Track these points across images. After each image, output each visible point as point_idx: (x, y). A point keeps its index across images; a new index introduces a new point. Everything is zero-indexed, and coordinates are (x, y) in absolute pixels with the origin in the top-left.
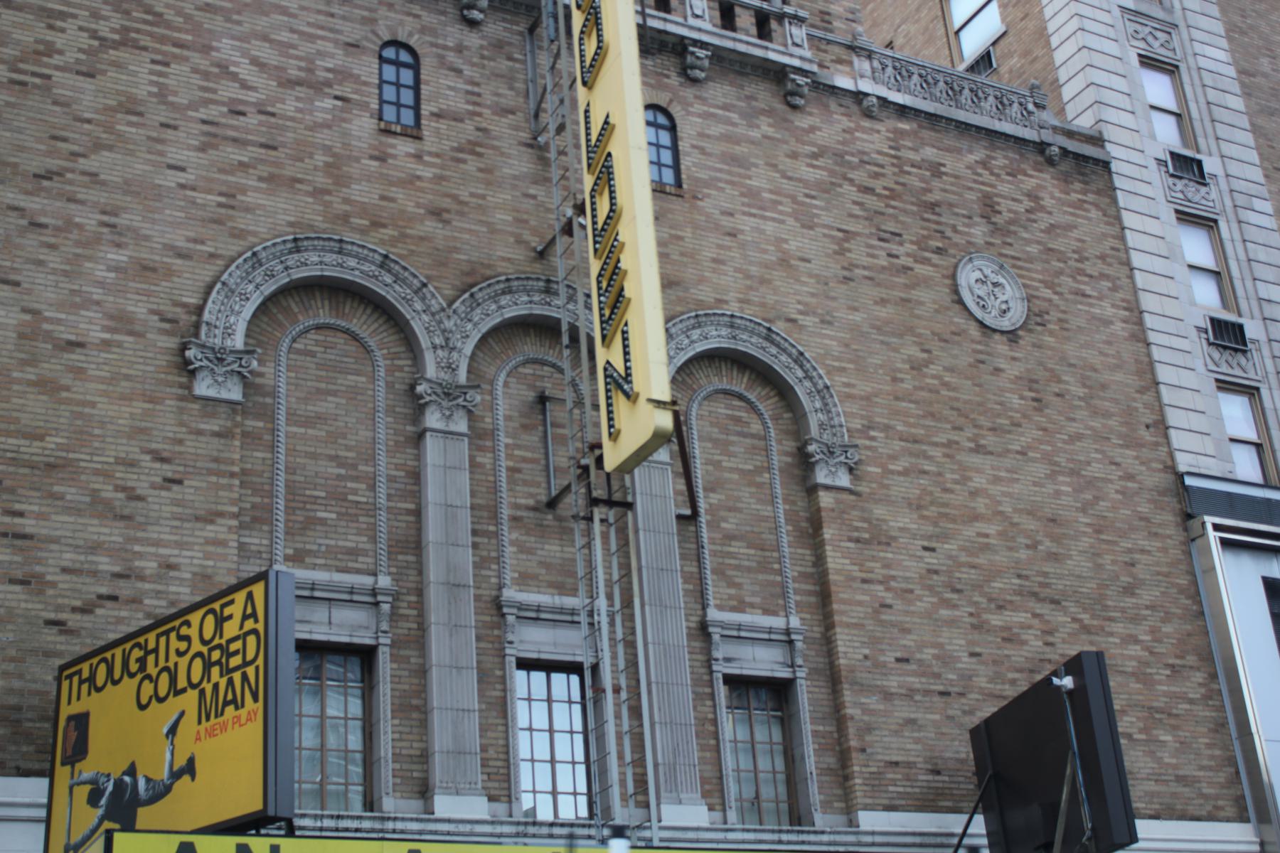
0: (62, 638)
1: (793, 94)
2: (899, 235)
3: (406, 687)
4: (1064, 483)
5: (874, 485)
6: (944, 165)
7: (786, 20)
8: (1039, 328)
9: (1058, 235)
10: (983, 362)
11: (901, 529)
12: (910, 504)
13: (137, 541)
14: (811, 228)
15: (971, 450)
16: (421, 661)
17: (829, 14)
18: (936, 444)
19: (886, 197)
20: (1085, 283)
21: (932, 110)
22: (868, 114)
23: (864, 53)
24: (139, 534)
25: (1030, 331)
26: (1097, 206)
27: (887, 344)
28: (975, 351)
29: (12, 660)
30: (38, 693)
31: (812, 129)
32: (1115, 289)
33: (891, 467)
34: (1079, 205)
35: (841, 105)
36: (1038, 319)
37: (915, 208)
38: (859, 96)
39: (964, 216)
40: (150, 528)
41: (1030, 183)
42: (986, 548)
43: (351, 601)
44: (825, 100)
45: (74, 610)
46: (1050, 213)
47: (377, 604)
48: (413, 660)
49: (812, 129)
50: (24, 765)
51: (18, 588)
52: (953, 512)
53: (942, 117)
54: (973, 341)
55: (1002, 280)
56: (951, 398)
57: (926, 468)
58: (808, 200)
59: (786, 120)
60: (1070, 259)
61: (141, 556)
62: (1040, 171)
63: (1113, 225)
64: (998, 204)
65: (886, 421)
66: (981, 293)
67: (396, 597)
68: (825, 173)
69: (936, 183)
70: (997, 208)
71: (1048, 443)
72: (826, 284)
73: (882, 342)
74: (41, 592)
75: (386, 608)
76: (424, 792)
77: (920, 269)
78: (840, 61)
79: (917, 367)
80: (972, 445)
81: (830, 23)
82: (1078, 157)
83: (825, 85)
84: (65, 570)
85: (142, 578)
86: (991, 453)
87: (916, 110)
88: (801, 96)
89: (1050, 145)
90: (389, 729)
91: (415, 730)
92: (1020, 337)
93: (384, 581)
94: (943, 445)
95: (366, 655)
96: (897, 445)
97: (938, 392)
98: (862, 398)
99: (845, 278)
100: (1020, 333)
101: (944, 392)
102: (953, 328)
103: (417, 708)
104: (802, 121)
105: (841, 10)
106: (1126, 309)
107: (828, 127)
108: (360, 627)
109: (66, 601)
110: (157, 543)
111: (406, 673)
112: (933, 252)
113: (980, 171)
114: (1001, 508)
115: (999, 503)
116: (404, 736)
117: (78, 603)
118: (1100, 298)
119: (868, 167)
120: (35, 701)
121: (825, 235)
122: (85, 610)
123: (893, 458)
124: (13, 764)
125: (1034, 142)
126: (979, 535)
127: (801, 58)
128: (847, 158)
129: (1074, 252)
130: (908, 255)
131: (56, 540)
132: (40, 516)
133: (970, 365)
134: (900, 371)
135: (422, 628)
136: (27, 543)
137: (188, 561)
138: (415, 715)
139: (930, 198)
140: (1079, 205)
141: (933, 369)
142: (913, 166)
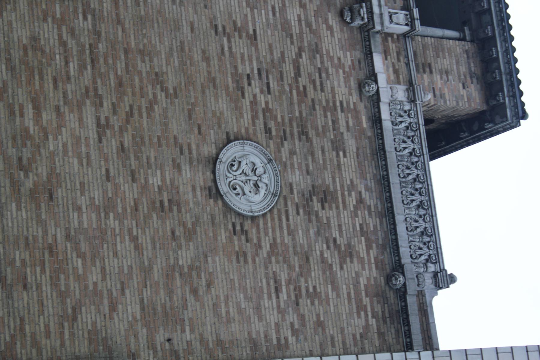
1: (351, 10)
2: (269, 93)
4: (90, 220)
5: (44, 7)
6: (345, 156)
7: (407, 13)
8: (230, 227)
9: (324, 273)
10: (182, 153)
11: (10, 23)
12: (34, 39)
14: (248, 5)
15: (98, 119)
17: (431, 72)
18: (95, 82)
19: (298, 88)
20: (289, 296)
21: (387, 148)
22: (361, 86)
23: (411, 94)
25: (225, 216)
26: (367, 326)
27: (172, 55)
28: (189, 145)
31: (330, 28)
32: (295, 332)
33: (64, 28)
34: (361, 308)
35: (359, 62)
36: (238, 228)
37: (297, 114)
38: (373, 77)
39: (307, 166)
41: (361, 247)
42: (12, 113)
44: (358, 47)
46: (342, 268)
49: (330, 28)
52: (37, 83)
53: (385, 160)
54: (198, 146)
55: (262, 192)
56: (140, 108)
57: (71, 65)
58: (270, 8)
59: (329, 5)
60: (306, 282)
62: (377, 267)
63: (355, 344)
64: (331, 208)
65: (103, 34)
66: (243, 166)
68: (298, 32)
69: (328, 145)
70: (326, 205)
71: (124, 209)
72: (206, 7)
73: (171, 49)
77: (246, 103)
78: (396, 72)
79: (158, 79)
80: (103, 122)
81: (424, 72)
82: (405, 310)
83: (370, 45)
86: (100, 141)
87: (382, 133)
88: (351, 19)
89: (404, 275)
92: (215, 201)
94: (96, 89)
96: (85, 40)
97: (142, 97)
98: (118, 15)
99: (216, 26)
100: (220, 202)
101: (144, 103)
102: (203, 129)
104: (333, 20)
105: (440, 86)
106: (278, 340)
107: (335, 42)
112: (265, 124)
113: (353, 193)
114: (50, 137)
115: (56, 139)
118: (280, 310)
119: (317, 75)
121: (246, 16)
123: (72, 32)
125: (400, 260)
126: (21, 107)
127: (381, 15)
128: (318, 56)
129: (314, 287)
130: (255, 96)
133: (175, 138)
134: (151, 61)
139: (312, 133)
140: (361, 308)
141: (161, 96)
142: (333, 122)
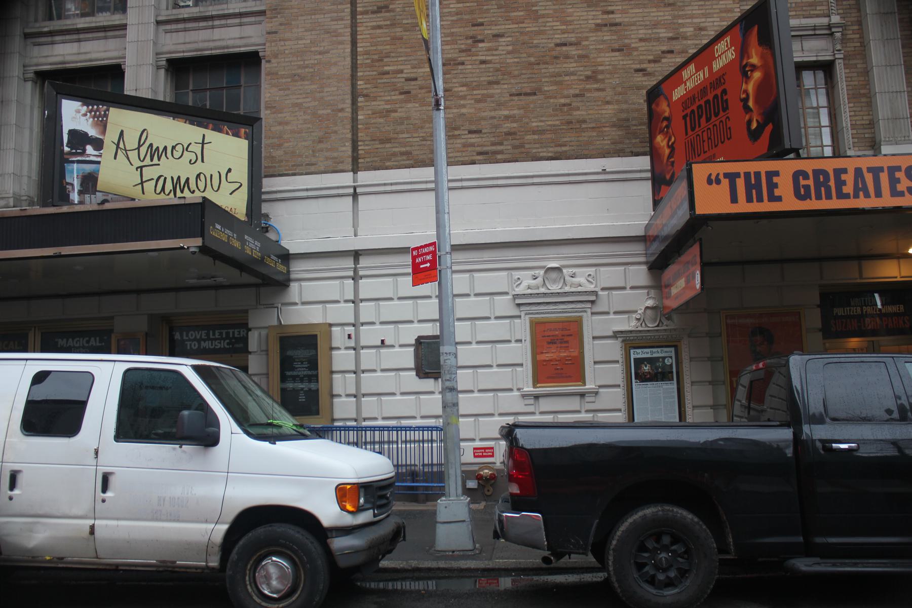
0: (645, 78)
3: (856, 83)
13: (680, 17)
16: (864, 66)
24: (681, 13)
29: (620, 94)
30: (637, 110)
40: (686, 8)
43: (815, 35)
45: (650, 61)
47: (832, 34)
48: (859, 66)
50: (634, 150)
51: (617, 54)
61: (683, 25)
67: (843, 27)
74: (630, 54)
75: (838, 35)
76: (874, 146)
84: (641, 40)
85: (686, 38)
90: (847, 110)
91: (864, 109)
93: (835, 19)
95: (827, 68)
103: (864, 95)
108: (822, 50)
109: (645, 57)
110: (692, 17)
111: (855, 74)
116: (857, 113)
117: (651, 57)
120: (636, 115)
122: (655, 61)
124: (629, 150)
131: (634, 24)
132: (624, 12)
135: (864, 46)
136: (619, 28)
137: (711, 24)
138: (863, 100)
